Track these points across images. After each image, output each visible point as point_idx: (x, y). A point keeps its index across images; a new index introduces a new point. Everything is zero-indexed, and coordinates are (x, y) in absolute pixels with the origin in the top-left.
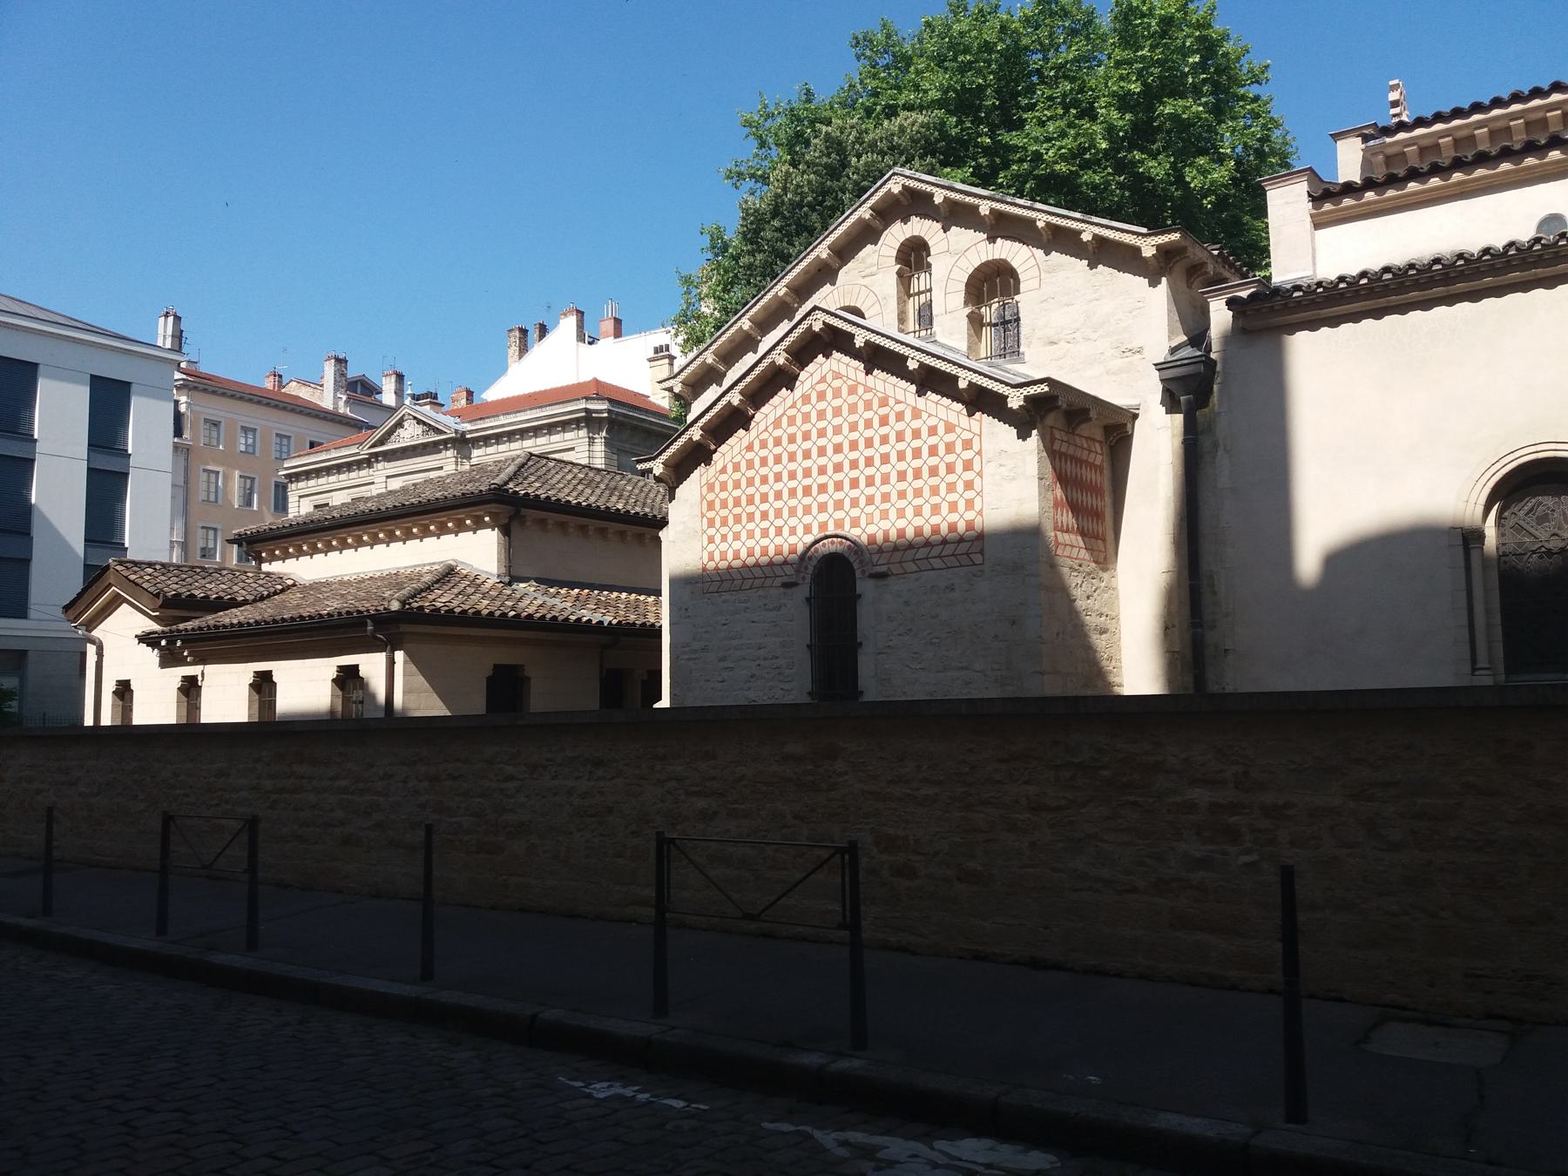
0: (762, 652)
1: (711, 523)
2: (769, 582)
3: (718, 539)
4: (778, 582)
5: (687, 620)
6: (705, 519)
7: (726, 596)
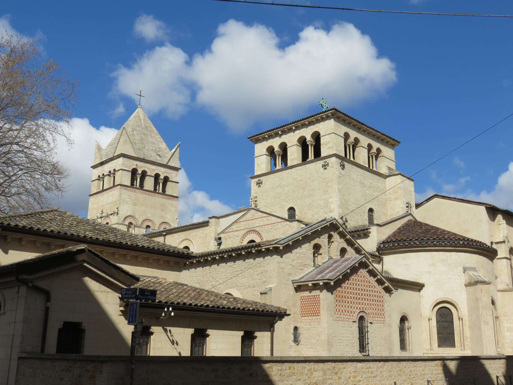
0: (348, 339)
2: (349, 320)
4: (352, 320)
5: (331, 327)
6: (335, 300)
7: (340, 322)
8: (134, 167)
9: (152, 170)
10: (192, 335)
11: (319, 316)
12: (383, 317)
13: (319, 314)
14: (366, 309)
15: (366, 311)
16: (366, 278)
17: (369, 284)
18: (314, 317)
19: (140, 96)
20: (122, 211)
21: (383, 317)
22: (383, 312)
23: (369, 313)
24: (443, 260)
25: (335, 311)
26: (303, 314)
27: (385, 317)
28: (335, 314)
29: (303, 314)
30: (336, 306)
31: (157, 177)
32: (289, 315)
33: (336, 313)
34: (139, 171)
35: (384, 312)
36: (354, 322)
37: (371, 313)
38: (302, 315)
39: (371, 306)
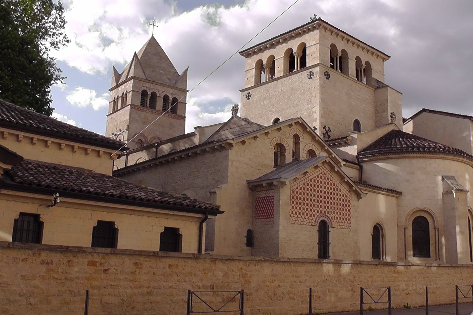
1: (293, 202)
2: (308, 224)
3: (295, 208)
4: (310, 224)
6: (291, 201)
8: (144, 88)
9: (161, 92)
10: (94, 228)
11: (273, 218)
12: (349, 222)
13: (272, 216)
14: (328, 213)
15: (329, 215)
16: (331, 180)
17: (334, 187)
18: (268, 219)
19: (154, 25)
20: (132, 129)
21: (349, 222)
22: (349, 217)
23: (332, 217)
24: (422, 168)
25: (291, 213)
26: (257, 216)
27: (350, 223)
28: (290, 216)
29: (257, 216)
30: (293, 207)
31: (166, 98)
32: (223, 212)
33: (292, 215)
34: (148, 93)
35: (351, 217)
36: (312, 225)
37: (334, 217)
38: (256, 218)
39: (334, 210)
